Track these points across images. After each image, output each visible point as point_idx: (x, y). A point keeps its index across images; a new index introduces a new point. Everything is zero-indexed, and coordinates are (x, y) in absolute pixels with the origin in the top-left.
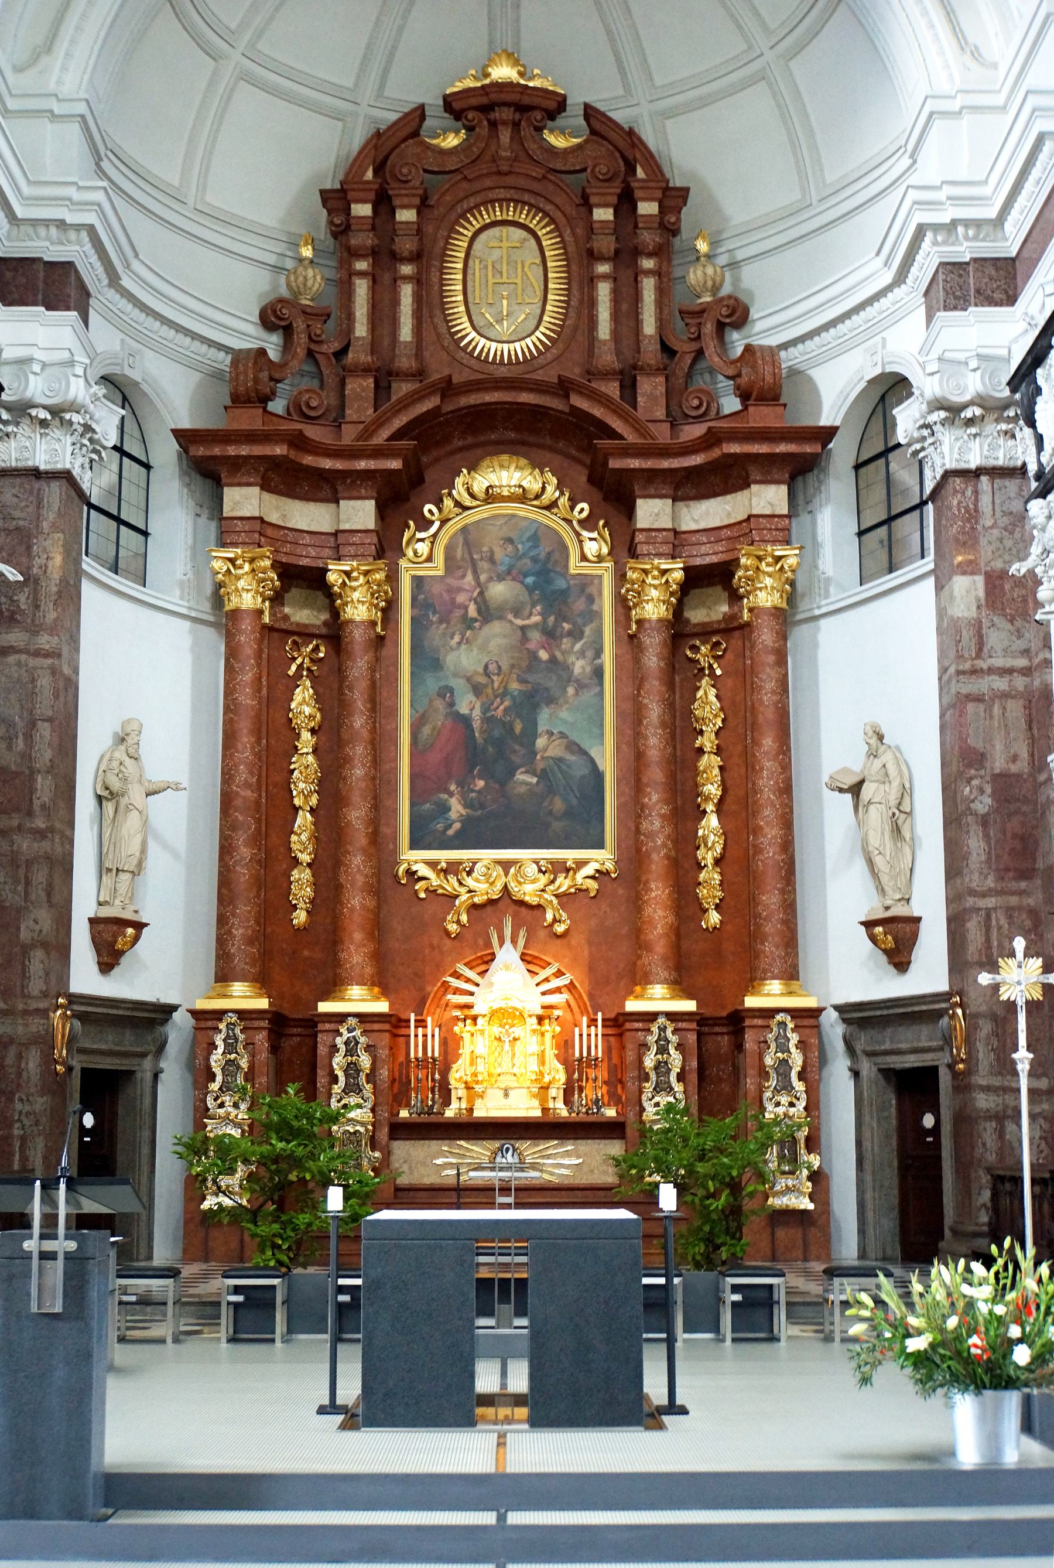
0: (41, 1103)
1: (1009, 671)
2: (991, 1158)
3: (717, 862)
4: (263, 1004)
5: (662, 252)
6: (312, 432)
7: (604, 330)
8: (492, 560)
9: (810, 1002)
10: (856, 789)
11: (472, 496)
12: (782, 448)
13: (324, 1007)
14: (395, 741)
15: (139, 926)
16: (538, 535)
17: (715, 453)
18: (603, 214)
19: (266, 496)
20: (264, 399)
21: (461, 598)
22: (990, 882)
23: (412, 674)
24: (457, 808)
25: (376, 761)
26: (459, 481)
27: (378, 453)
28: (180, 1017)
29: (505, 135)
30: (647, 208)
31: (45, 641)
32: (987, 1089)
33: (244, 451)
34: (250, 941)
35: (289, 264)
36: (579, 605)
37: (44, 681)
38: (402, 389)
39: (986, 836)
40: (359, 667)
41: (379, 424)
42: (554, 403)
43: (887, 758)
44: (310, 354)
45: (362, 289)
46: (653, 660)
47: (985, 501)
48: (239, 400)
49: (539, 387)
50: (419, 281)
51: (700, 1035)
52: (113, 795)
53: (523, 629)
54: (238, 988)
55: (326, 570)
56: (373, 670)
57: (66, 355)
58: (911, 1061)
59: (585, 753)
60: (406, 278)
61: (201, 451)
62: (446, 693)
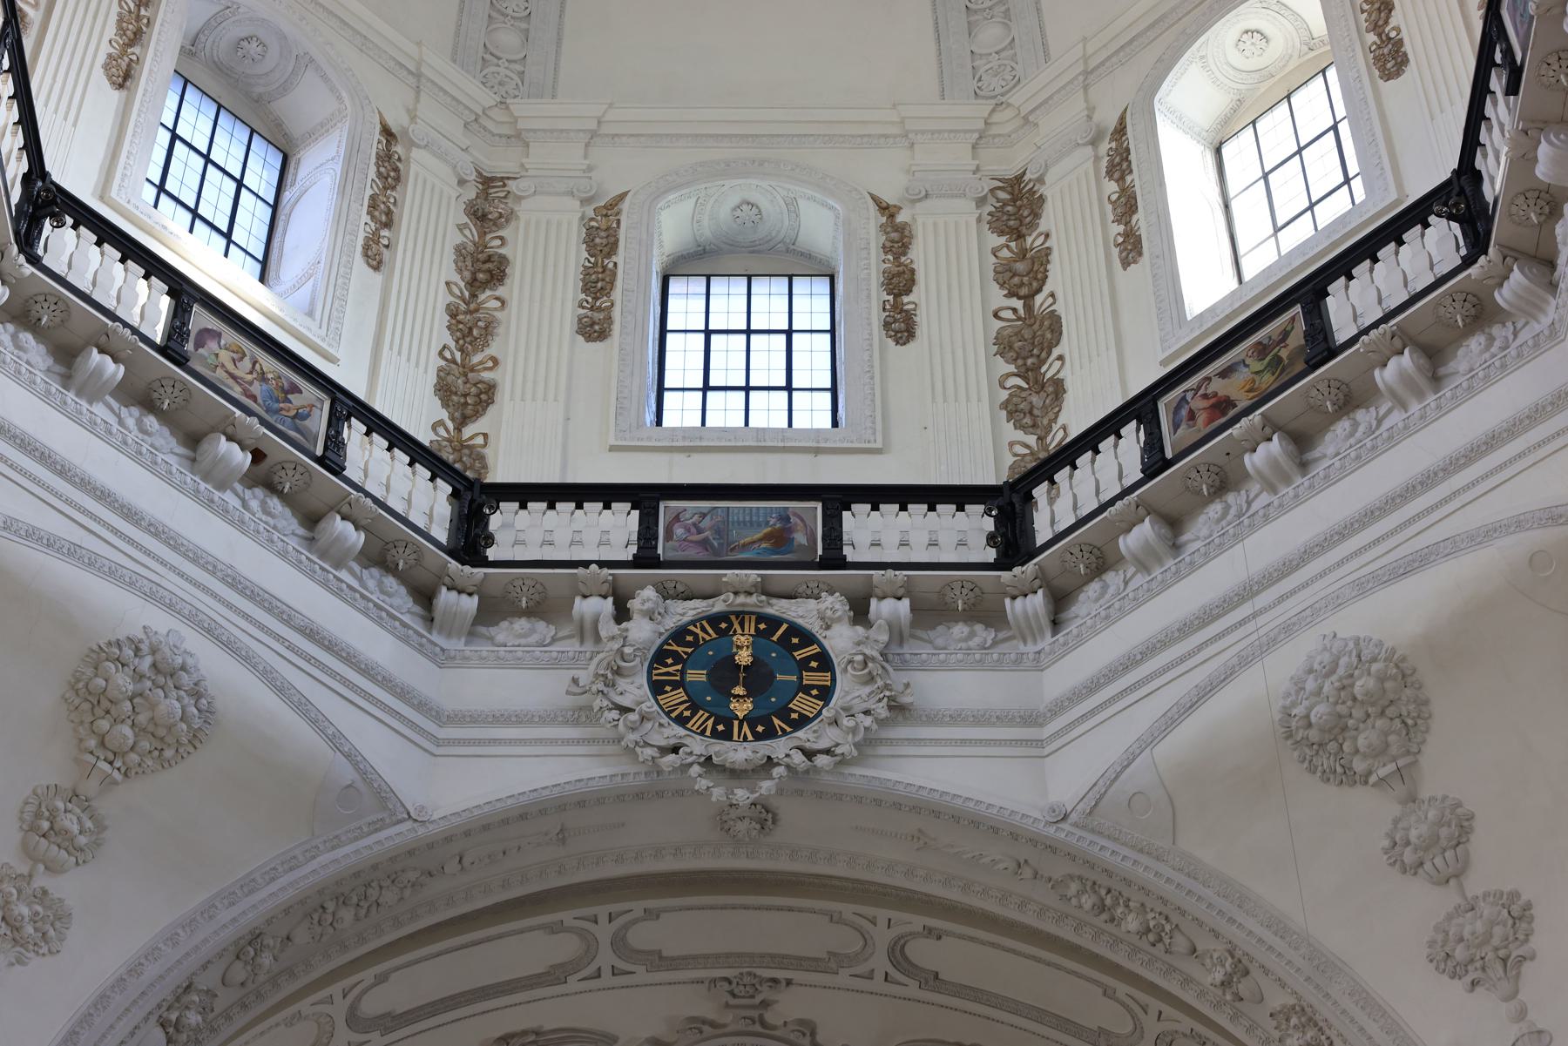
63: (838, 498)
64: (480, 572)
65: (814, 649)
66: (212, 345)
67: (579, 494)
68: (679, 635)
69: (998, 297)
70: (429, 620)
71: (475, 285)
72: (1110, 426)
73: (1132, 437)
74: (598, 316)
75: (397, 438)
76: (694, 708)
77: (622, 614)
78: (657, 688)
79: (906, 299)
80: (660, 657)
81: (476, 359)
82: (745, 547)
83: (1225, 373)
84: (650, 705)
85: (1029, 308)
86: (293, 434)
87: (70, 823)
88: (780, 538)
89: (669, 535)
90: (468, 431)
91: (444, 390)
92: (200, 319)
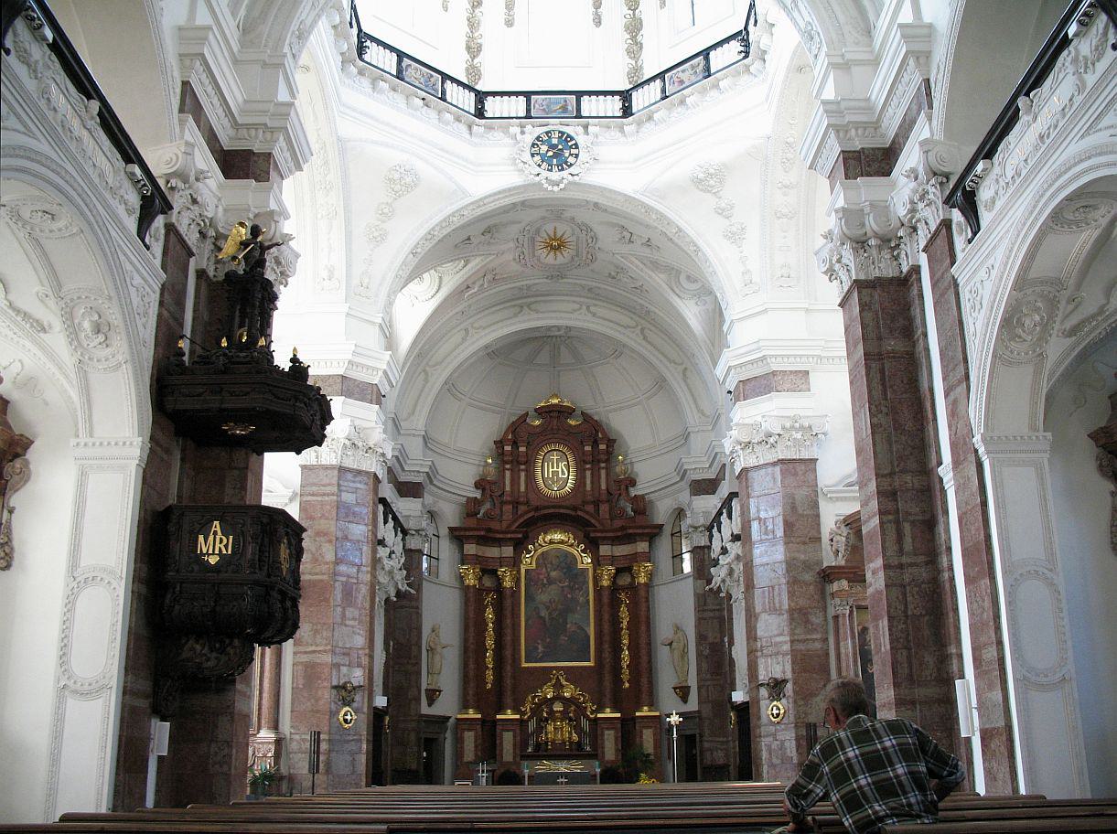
0: (415, 749)
1: (711, 611)
2: (709, 763)
3: (627, 666)
4: (479, 716)
5: (607, 461)
6: (495, 525)
7: (588, 487)
8: (551, 564)
9: (658, 714)
10: (670, 644)
11: (545, 542)
12: (646, 531)
13: (498, 717)
14: (520, 626)
15: (440, 691)
16: (568, 554)
17: (625, 532)
18: (588, 448)
19: (478, 547)
20: (476, 515)
21: (541, 577)
22: (709, 676)
23: (526, 606)
24: (541, 648)
25: (514, 634)
26: (540, 538)
27: (513, 532)
28: (451, 720)
29: (555, 422)
30: (603, 447)
31: (414, 603)
32: (707, 741)
33: (471, 533)
34: (474, 696)
35: (482, 463)
36: (581, 579)
37: (414, 617)
38: (522, 508)
39: (708, 662)
40: (508, 603)
41: (515, 521)
42: (573, 513)
43: (680, 634)
44: (491, 495)
45: (508, 474)
46: (606, 600)
47: (706, 557)
48: (468, 515)
49: (567, 508)
50: (526, 470)
51: (622, 724)
52: (432, 649)
53: (563, 587)
54: (471, 711)
55: (497, 571)
56: (513, 603)
57: (419, 514)
58: (688, 733)
59: (583, 630)
60: (522, 470)
61: (457, 533)
62: (537, 608)
63: (579, 94)
64: (484, 121)
65: (574, 142)
66: (409, 70)
67: (509, 94)
68: (538, 139)
69: (626, 11)
70: (471, 134)
71: (473, 7)
72: (653, 79)
73: (658, 83)
74: (510, 18)
75: (459, 83)
76: (543, 162)
77: (523, 133)
78: (533, 155)
79: (599, 10)
80: (533, 145)
81: (476, 35)
82: (555, 111)
83: (683, 71)
84: (531, 162)
85: (634, 15)
86: (433, 92)
87: (386, 211)
88: (564, 109)
89: (534, 106)
90: (476, 61)
91: (468, 48)
92: (406, 61)
